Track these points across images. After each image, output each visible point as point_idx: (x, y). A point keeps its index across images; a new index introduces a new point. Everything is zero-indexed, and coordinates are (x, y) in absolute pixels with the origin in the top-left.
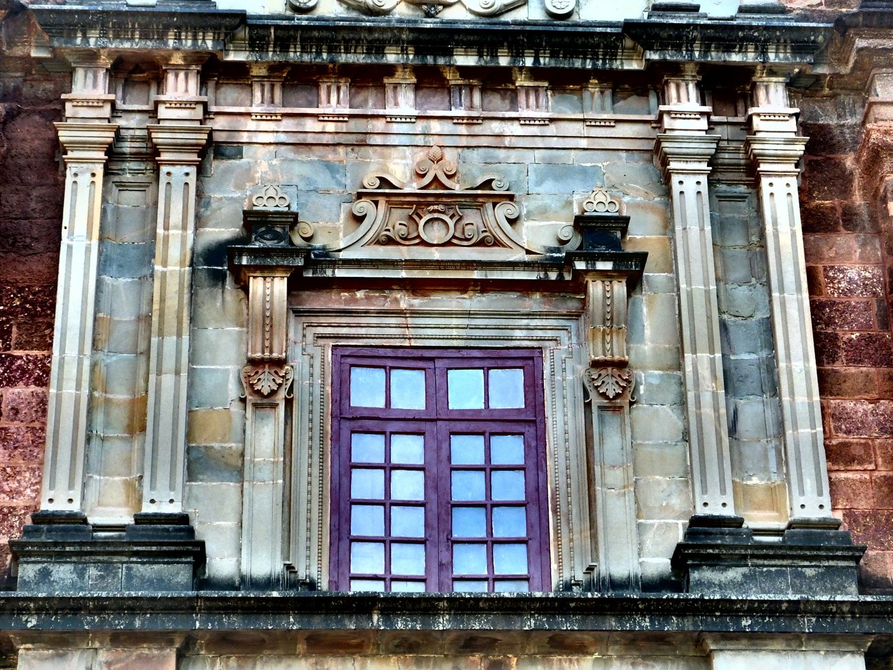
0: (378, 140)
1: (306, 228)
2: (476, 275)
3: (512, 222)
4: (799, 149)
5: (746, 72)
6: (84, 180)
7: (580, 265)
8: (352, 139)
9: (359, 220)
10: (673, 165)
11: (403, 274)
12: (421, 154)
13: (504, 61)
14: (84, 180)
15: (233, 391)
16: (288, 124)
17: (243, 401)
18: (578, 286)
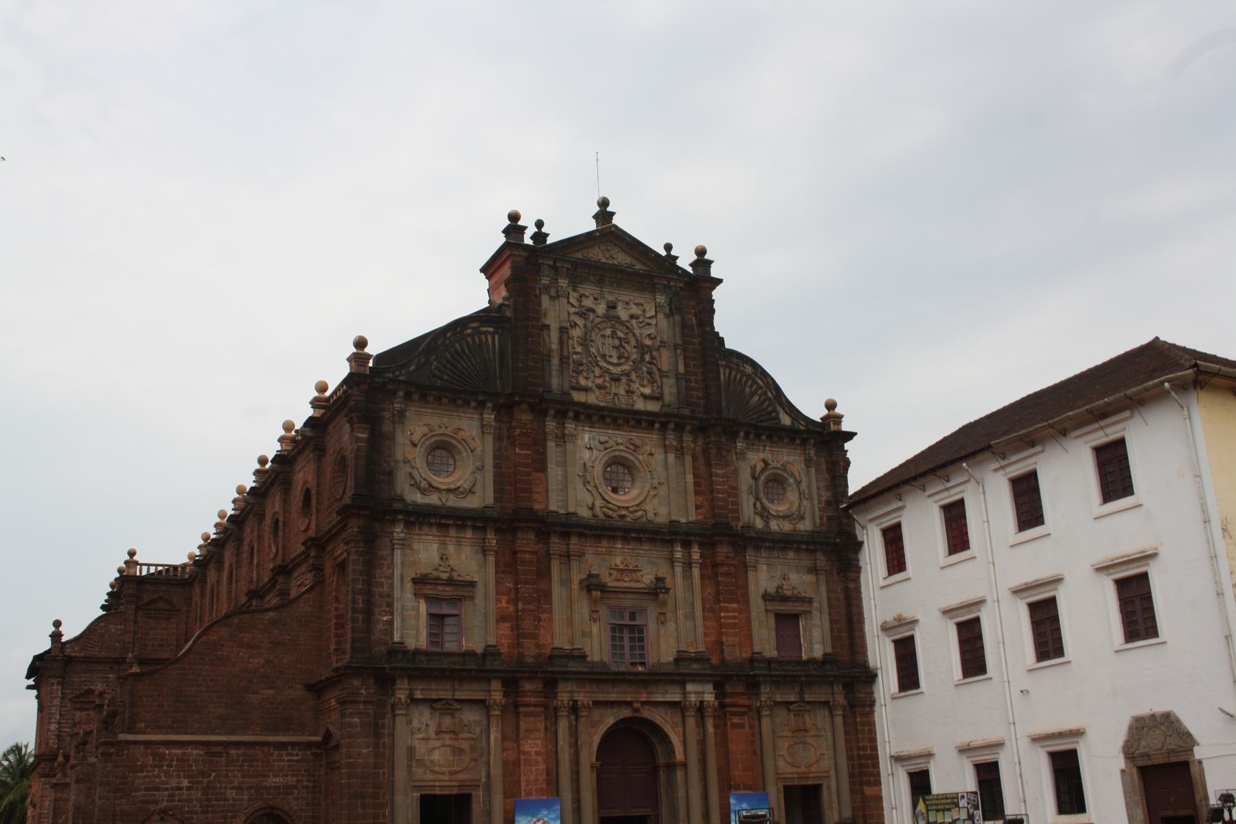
0: (613, 553)
1: (601, 577)
2: (636, 590)
3: (642, 576)
4: (701, 561)
5: (690, 541)
6: (555, 563)
7: (658, 591)
8: (608, 553)
9: (611, 575)
10: (675, 564)
11: (621, 590)
12: (622, 557)
13: (641, 536)
14: (555, 563)
15: (587, 616)
16: (595, 549)
17: (590, 620)
18: (656, 594)
